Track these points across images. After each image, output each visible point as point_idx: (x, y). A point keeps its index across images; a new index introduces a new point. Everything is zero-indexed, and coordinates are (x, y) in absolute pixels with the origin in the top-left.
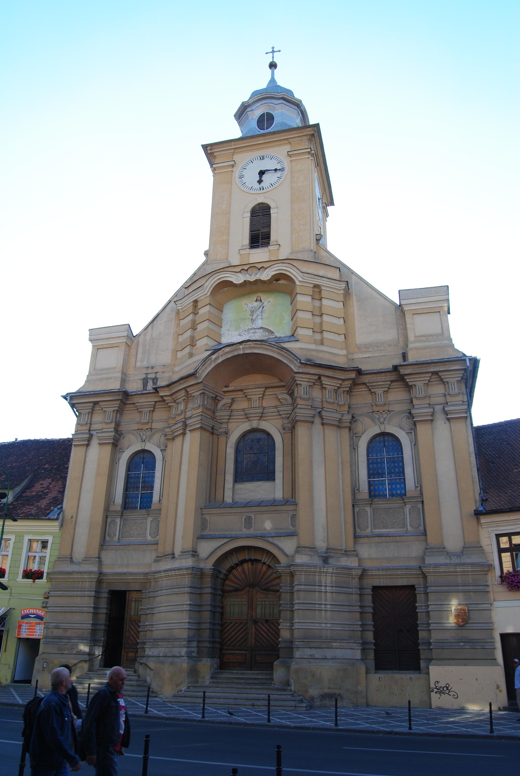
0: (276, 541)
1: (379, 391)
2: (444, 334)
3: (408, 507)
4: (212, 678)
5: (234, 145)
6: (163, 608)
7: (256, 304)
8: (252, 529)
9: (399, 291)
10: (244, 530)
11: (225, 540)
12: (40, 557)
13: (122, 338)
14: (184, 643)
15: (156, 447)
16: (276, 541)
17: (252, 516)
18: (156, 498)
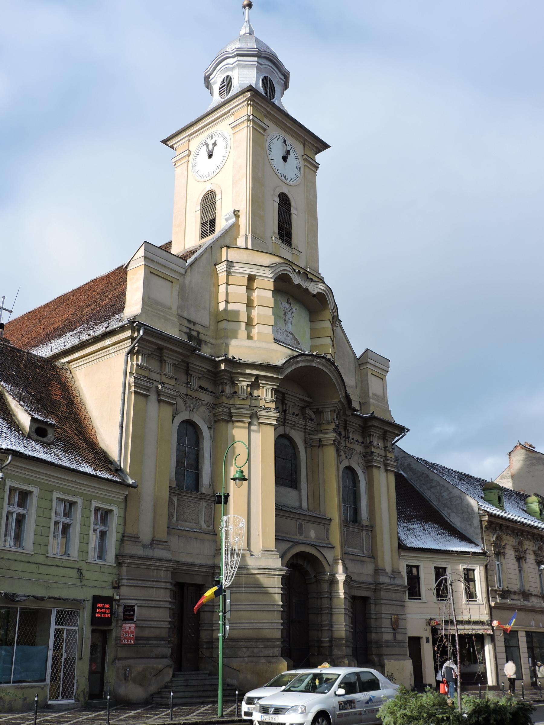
0: (322, 550)
1: (351, 430)
2: (383, 398)
3: (364, 533)
4: (395, 683)
5: (270, 109)
6: (243, 607)
7: (287, 306)
8: (303, 536)
9: (367, 350)
10: (298, 535)
11: (291, 544)
12: (18, 515)
13: (177, 274)
14: (278, 643)
15: (203, 422)
16: (322, 550)
17: (303, 523)
18: (205, 480)
